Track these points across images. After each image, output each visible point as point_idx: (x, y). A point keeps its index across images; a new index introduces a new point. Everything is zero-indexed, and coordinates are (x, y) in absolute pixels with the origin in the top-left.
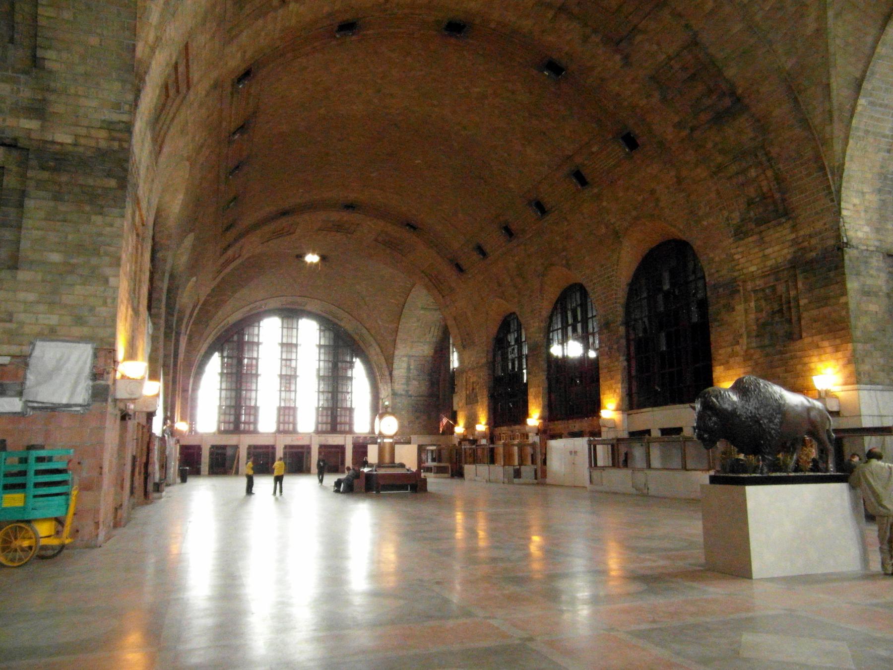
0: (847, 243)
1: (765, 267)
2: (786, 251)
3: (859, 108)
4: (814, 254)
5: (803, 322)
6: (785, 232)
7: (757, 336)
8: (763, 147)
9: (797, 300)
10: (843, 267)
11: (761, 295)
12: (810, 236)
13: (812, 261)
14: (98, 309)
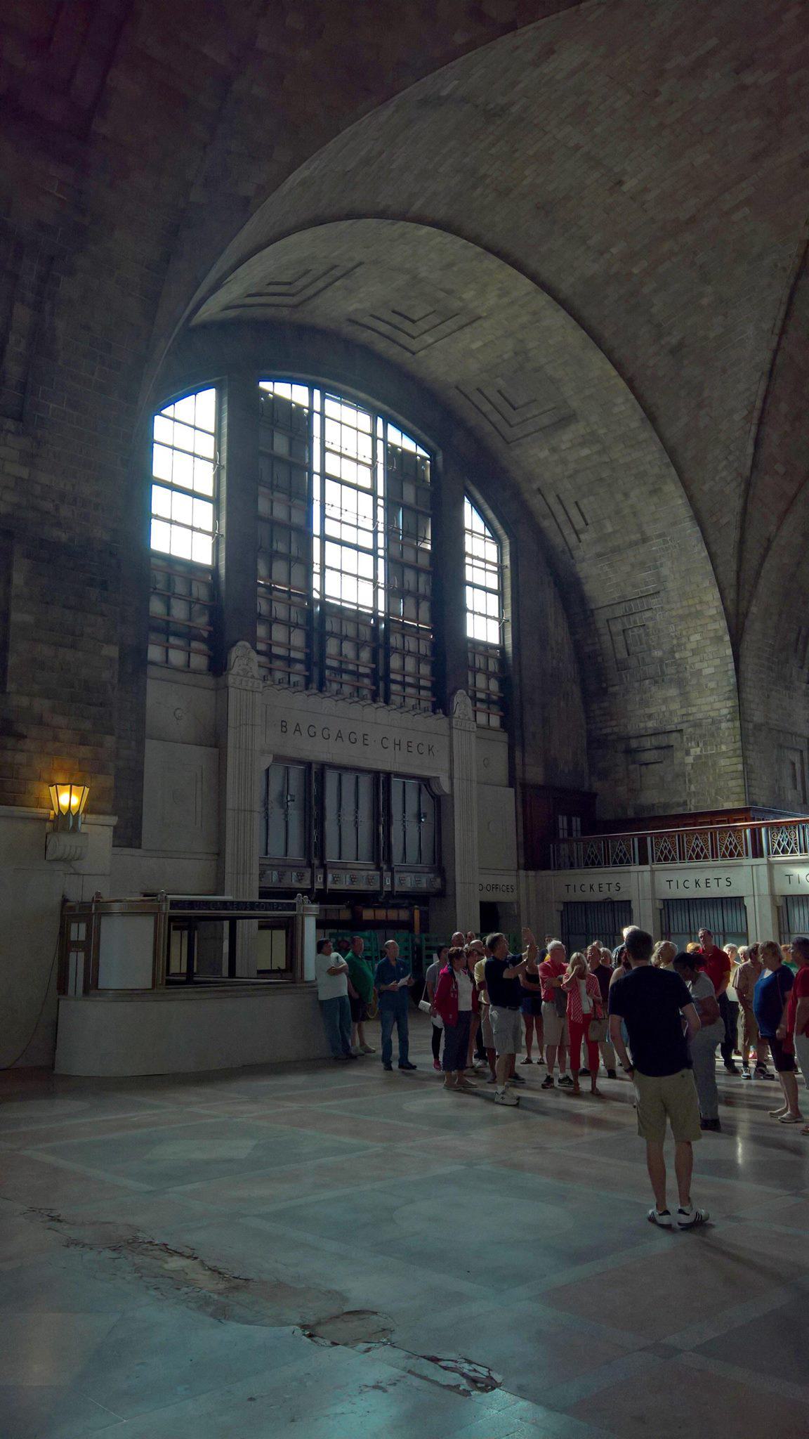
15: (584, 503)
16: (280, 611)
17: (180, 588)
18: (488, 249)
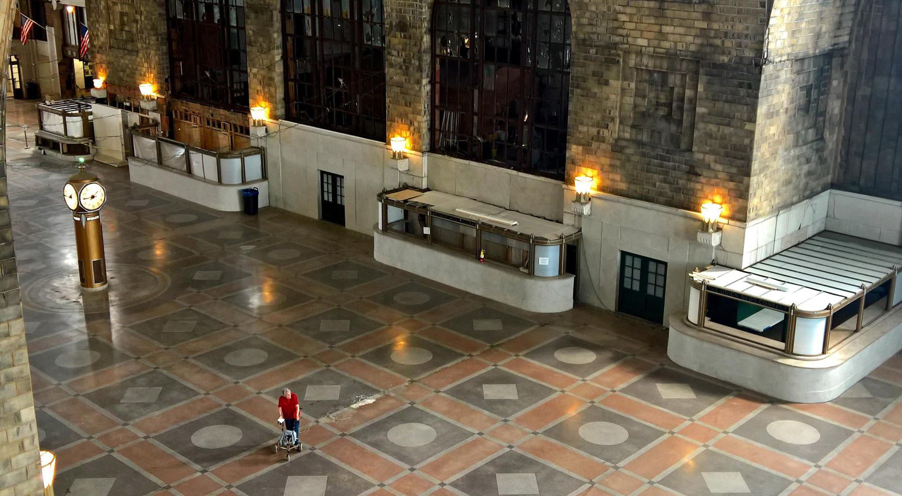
2: (690, 39)
4: (726, 59)
5: (696, 134)
6: (695, 15)
7: (633, 127)
9: (693, 102)
10: (758, 89)
11: (646, 76)
12: (726, 34)
13: (723, 66)
14: (13, 460)
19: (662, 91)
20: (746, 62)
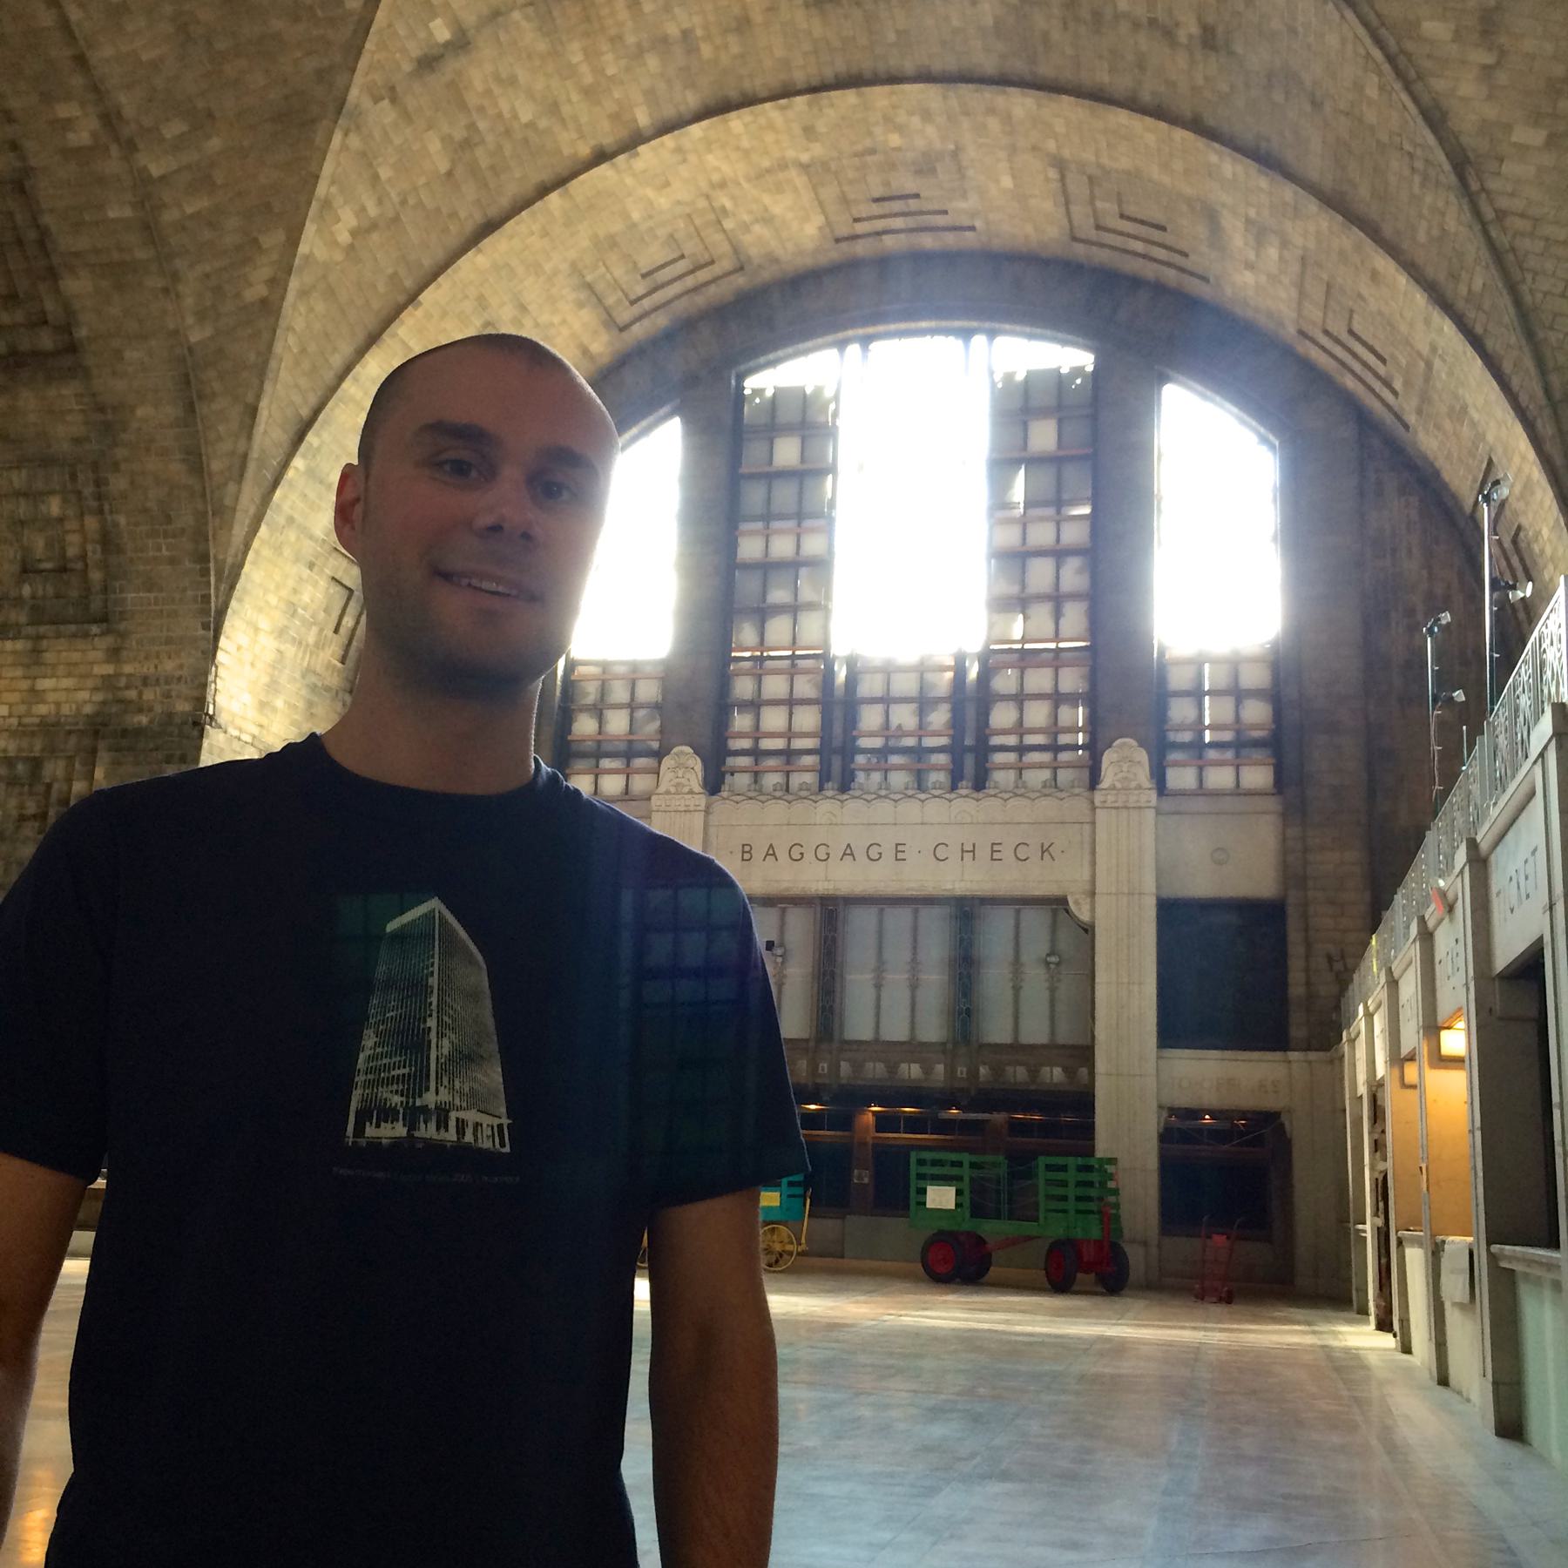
0: (212, 718)
1: (29, 714)
2: (83, 695)
3: (290, 474)
4: (144, 720)
6: (92, 655)
8: (95, 466)
12: (145, 681)
13: (139, 732)
15: (1357, 327)
16: (775, 686)
17: (619, 694)
18: (816, 89)
19: (31, 794)
20: (177, 720)
